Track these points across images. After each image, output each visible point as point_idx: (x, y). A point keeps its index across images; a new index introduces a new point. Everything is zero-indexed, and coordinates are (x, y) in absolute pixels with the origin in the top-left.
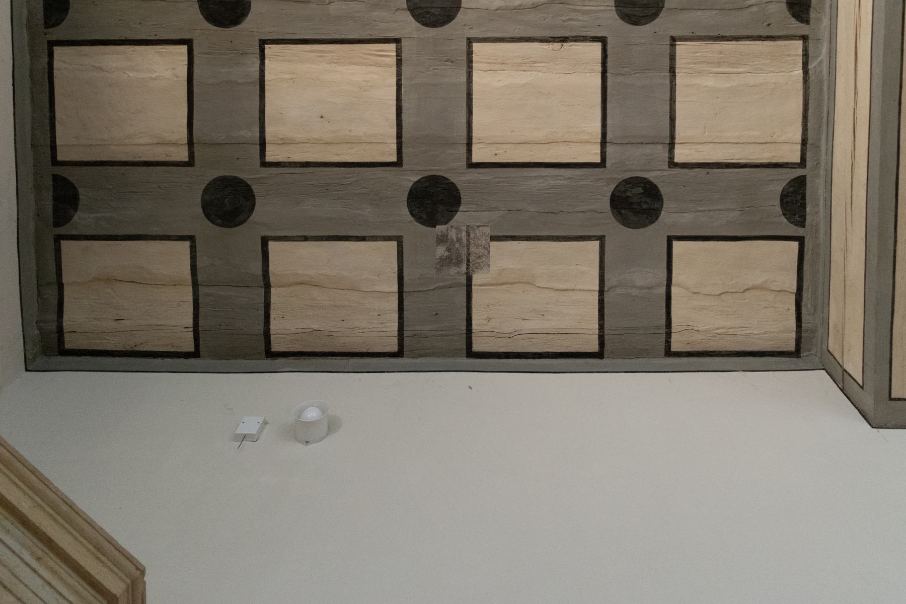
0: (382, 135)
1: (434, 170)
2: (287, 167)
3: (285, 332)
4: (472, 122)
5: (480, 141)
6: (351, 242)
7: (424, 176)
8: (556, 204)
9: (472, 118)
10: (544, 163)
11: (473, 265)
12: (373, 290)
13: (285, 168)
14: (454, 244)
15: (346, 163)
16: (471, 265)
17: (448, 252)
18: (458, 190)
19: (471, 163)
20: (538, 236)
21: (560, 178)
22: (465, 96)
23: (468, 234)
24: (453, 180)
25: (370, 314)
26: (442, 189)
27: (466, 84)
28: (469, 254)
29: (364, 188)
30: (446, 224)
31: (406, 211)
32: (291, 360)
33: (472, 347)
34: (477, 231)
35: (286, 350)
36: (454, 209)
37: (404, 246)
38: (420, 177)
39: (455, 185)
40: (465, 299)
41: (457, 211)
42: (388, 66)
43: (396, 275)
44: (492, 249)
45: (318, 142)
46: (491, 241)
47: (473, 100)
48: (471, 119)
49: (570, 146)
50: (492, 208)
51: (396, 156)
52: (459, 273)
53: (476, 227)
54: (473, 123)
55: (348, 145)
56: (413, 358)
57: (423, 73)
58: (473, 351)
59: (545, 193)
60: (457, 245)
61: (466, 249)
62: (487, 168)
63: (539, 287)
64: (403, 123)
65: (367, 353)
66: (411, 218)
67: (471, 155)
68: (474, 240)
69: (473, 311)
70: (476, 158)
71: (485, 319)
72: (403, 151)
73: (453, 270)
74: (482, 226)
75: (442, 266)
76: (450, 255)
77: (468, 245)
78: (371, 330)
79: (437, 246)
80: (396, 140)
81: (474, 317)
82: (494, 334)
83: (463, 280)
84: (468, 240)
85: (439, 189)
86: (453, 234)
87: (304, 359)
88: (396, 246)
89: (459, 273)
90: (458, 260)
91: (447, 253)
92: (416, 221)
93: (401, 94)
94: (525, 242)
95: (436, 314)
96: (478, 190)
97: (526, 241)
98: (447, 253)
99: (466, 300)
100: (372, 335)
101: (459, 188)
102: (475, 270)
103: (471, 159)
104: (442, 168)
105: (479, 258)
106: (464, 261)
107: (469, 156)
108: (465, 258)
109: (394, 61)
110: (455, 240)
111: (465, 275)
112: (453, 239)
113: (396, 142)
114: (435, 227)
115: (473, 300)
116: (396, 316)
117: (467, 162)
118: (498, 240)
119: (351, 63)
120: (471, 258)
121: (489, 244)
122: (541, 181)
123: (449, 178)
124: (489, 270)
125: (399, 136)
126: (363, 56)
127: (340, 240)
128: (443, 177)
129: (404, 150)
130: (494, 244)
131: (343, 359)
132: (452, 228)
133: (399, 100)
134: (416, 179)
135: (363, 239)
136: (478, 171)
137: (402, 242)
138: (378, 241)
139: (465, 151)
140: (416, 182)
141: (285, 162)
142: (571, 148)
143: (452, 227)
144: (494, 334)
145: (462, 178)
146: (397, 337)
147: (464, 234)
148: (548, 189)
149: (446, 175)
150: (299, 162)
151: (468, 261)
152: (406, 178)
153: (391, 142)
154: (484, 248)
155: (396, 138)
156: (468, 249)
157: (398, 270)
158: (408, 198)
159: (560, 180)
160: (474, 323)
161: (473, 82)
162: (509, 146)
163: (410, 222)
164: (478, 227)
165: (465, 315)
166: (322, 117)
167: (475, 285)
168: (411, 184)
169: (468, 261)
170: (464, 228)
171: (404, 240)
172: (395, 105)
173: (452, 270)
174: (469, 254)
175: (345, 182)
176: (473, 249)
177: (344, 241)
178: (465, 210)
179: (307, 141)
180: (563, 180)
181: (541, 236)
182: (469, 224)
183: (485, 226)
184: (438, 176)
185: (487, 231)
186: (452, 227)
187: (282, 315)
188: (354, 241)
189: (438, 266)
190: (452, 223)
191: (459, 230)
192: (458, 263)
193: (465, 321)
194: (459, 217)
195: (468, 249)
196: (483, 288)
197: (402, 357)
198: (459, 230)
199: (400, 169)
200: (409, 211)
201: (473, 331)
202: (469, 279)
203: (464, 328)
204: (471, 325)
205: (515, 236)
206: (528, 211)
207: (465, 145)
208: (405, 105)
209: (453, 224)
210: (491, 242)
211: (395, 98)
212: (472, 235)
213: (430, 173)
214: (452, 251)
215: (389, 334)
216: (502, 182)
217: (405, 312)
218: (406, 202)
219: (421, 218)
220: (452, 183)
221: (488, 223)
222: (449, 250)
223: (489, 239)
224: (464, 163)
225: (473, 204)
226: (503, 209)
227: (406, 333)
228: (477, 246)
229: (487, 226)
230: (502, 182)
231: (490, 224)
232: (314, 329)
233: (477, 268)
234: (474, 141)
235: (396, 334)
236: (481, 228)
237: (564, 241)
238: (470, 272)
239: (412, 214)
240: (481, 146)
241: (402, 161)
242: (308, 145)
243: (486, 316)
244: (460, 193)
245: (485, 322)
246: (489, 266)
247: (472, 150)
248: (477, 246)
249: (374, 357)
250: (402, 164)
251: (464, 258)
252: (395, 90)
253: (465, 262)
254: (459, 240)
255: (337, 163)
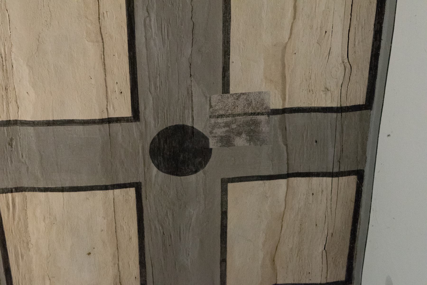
0: (105, 203)
1: (143, 152)
2: (146, 278)
3: (325, 270)
4: (82, 120)
5: (105, 110)
6: (228, 223)
7: (151, 161)
8: (182, 25)
9: (76, 120)
10: (128, 41)
11: (258, 109)
12: (283, 199)
13: (148, 281)
14: (233, 129)
15: (138, 231)
16: (259, 111)
17: (241, 134)
18: (167, 128)
19: (132, 118)
20: (224, 43)
21: (147, 22)
22: (51, 128)
23: (222, 116)
24: (155, 134)
25: (311, 202)
26: (166, 143)
27: (37, 127)
28: (245, 114)
29: (167, 215)
30: (206, 139)
31: (192, 178)
32: (356, 265)
33: (359, 105)
34: (217, 107)
35: (345, 269)
36: (190, 131)
37: (233, 176)
38: (152, 165)
39: (161, 131)
40: (300, 115)
41: (193, 127)
42: (25, 199)
43: (267, 182)
44: (240, 91)
45: (117, 257)
46: (229, 93)
47: (55, 119)
48: (78, 121)
49: (105, 12)
50: (188, 93)
51: (128, 189)
52: (268, 122)
53: (211, 109)
54: (83, 119)
55: (119, 231)
56: (366, 161)
57: (28, 168)
58: (364, 104)
59: (168, 38)
60: (234, 126)
61: (238, 117)
62: (138, 101)
63: (290, 38)
64: (89, 185)
65: (355, 203)
66: (201, 173)
67: (123, 118)
68: (228, 110)
69: (316, 106)
70: (127, 112)
71: (326, 94)
72: (122, 183)
73: (265, 128)
74: (210, 103)
75: (258, 140)
76: (245, 132)
77: (234, 116)
78: (329, 201)
79: (235, 146)
80: (110, 191)
81: (323, 105)
82: (345, 84)
83: (276, 118)
84: (228, 116)
85: (166, 146)
86: (220, 132)
87: (356, 254)
88: (233, 184)
89: (268, 122)
90: (253, 124)
91: (244, 135)
92: (203, 168)
93: (55, 188)
94: (231, 56)
95: (316, 142)
96: (166, 109)
97: (229, 55)
98: (244, 135)
99: (302, 114)
100: (334, 198)
101: (165, 127)
102: (264, 107)
103: (128, 117)
104: (141, 145)
105: (250, 104)
106: (253, 118)
107: (124, 120)
108: (249, 118)
109: (18, 196)
110: (227, 129)
111: (271, 116)
112: (227, 131)
113: (112, 191)
114: (211, 149)
115: (301, 106)
116: (315, 180)
117: (132, 122)
118: (228, 85)
119: (26, 231)
120: (250, 112)
121: (232, 95)
122: (152, 43)
123: (152, 138)
124: (265, 93)
125: (106, 188)
126: (16, 222)
127: (226, 232)
128: (152, 143)
129: (122, 182)
130: (233, 89)
131: (360, 222)
132: (212, 133)
133: (63, 190)
134: (155, 170)
135: (224, 214)
136: (143, 109)
137: (229, 179)
138: (227, 200)
139: (119, 124)
140: (158, 169)
141: (141, 280)
142: (107, 12)
143: (211, 133)
144: (345, 84)
145: (152, 125)
146: (340, 178)
147: (220, 120)
148: (162, 35)
149: (149, 140)
150: (140, 270)
151: (252, 114)
152: (154, 178)
153: (112, 195)
154: (237, 99)
155: (107, 191)
156: (239, 115)
157: (261, 180)
158: (177, 175)
159: (150, 20)
160: (329, 105)
161: (33, 120)
162: (108, 79)
163: (205, 174)
164: (211, 106)
165: (319, 115)
166: (89, 254)
167: (284, 104)
168: (161, 173)
169: (252, 114)
170: (213, 121)
171: (226, 177)
172: (68, 193)
173: (264, 129)
174: (245, 114)
175: (160, 232)
176: (239, 110)
177: (226, 229)
178: (191, 120)
179: (116, 265)
180: (150, 18)
181: (224, 39)
182: (208, 116)
183: (210, 100)
184: (151, 148)
185: (215, 98)
186: (211, 133)
187: (307, 274)
188: (227, 221)
189: (258, 143)
190: (206, 133)
191: (214, 127)
192: (256, 124)
193: (326, 114)
194: (199, 127)
195: (239, 115)
196: (287, 97)
197: (363, 171)
198: (214, 127)
199: (143, 184)
200: (192, 174)
201: (339, 106)
202: (275, 112)
203: (334, 115)
204: (332, 108)
205: (224, 68)
206: (191, 55)
207: (111, 124)
208: (67, 184)
209: (208, 131)
210: (230, 93)
211: (61, 193)
212: (221, 112)
213: (148, 156)
214: (240, 130)
215: (335, 185)
216: (155, 84)
217: (311, 171)
218: (182, 177)
219: (200, 163)
220: (158, 135)
221: (206, 97)
222: (239, 134)
223: (226, 95)
224: (134, 125)
225: (184, 113)
226: (189, 82)
227: (336, 170)
228: (235, 106)
229: (210, 98)
230: (155, 84)
231: (208, 96)
232: (323, 249)
233: (263, 105)
234: (105, 116)
235: (335, 179)
236: (213, 104)
237: (230, 13)
238: (266, 111)
239: (196, 172)
240: (111, 110)
241: (133, 183)
242: (120, 264)
243: (322, 93)
244: (170, 127)
245: (329, 94)
246: (260, 93)
247: (117, 118)
248: (235, 106)
249: (361, 195)
250: (137, 183)
251: (249, 119)
252: (51, 193)
253: (254, 117)
254: (227, 125)
255: (139, 239)
